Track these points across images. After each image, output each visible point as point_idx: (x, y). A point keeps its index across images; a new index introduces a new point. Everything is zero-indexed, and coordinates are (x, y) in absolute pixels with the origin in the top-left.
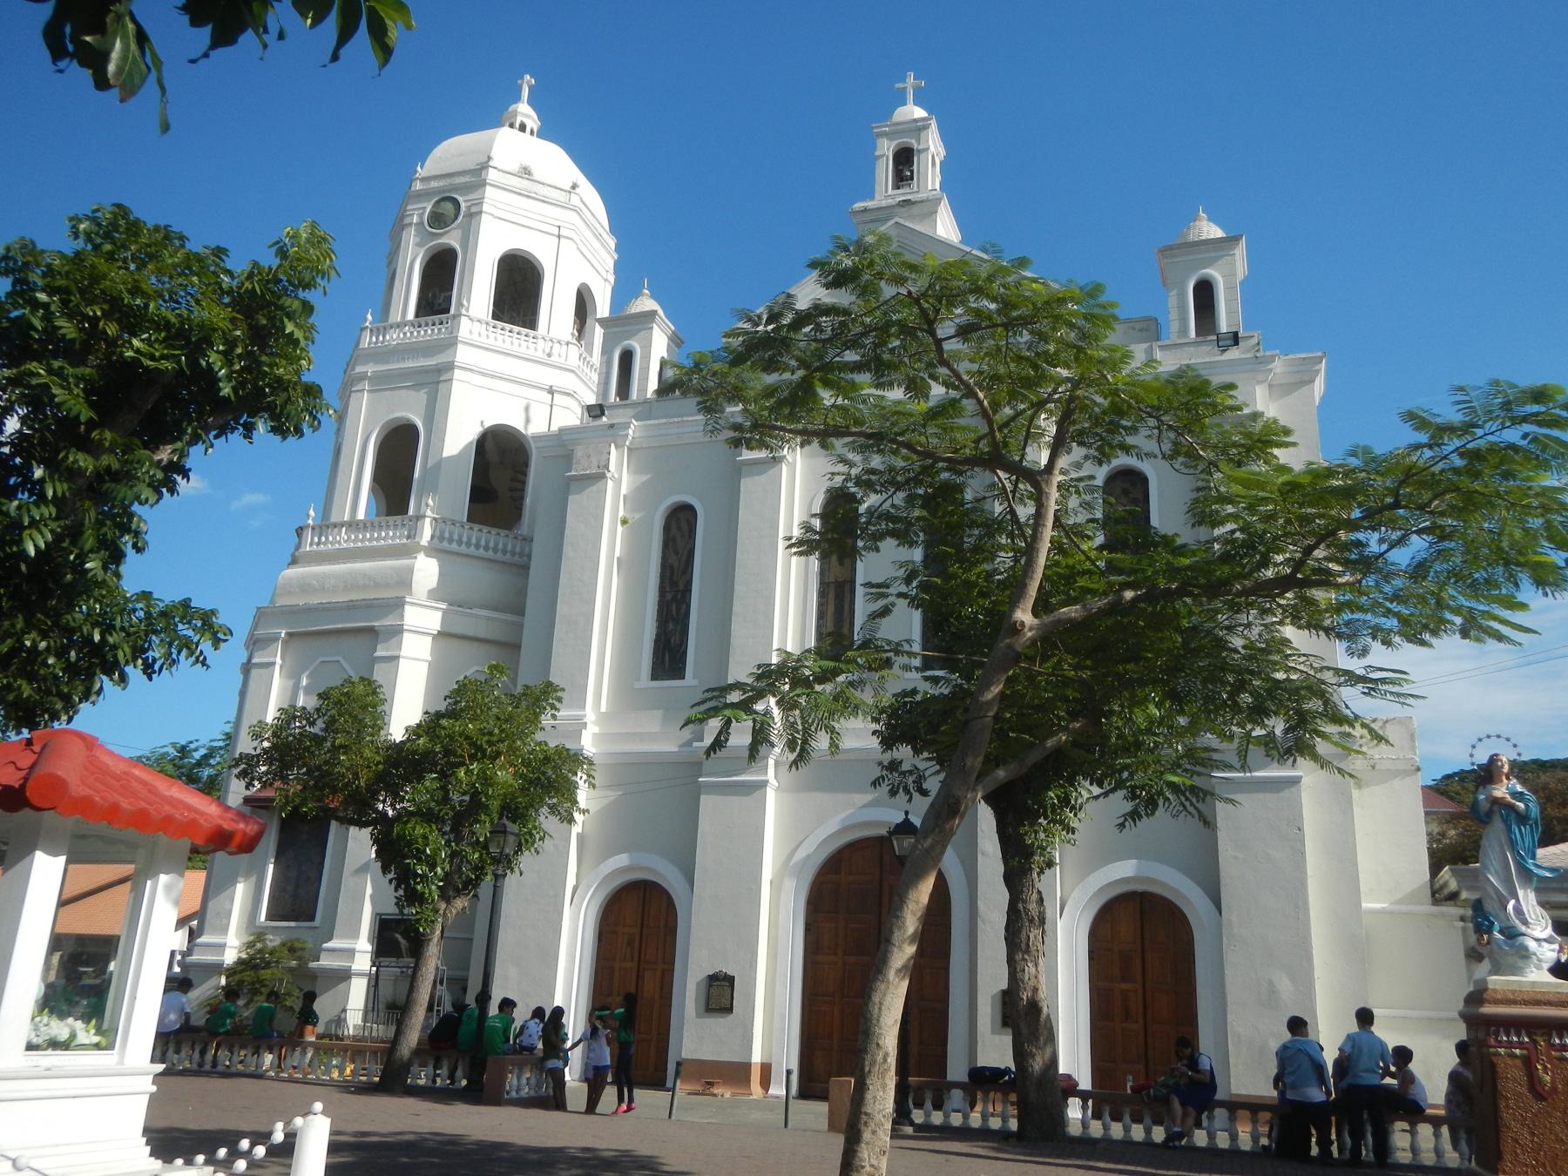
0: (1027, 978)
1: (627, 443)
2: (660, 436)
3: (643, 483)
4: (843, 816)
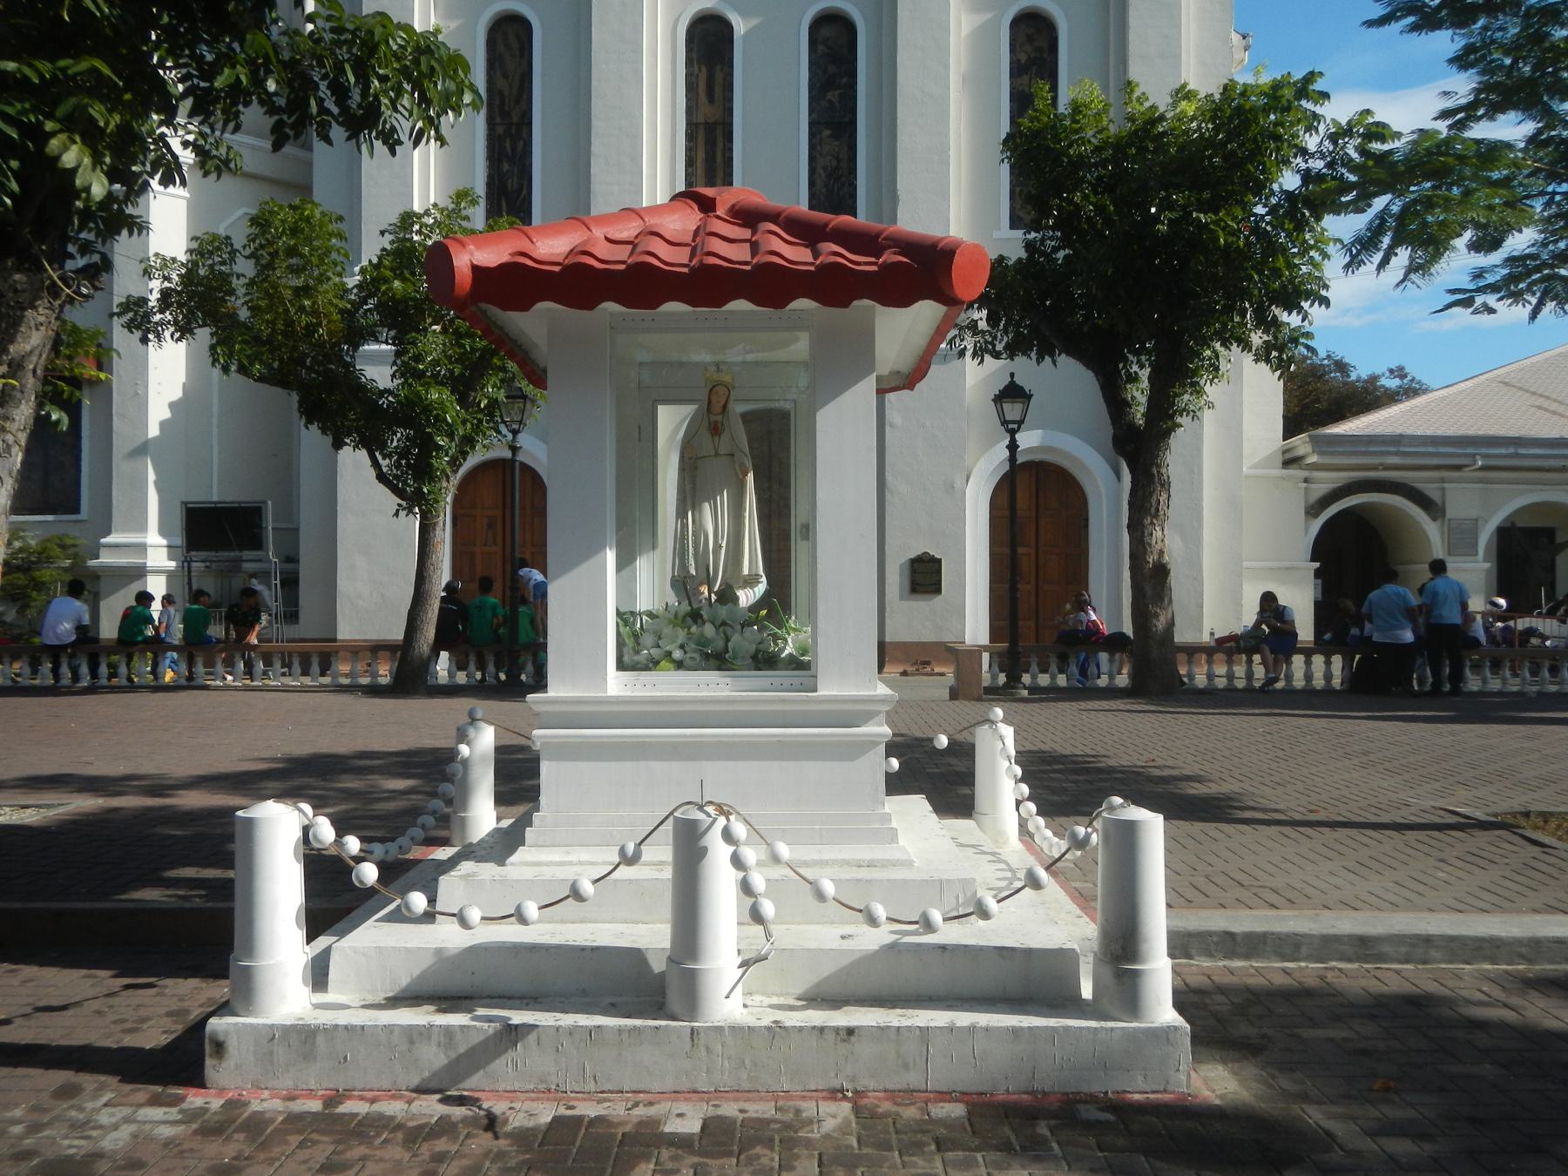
0: (1154, 542)
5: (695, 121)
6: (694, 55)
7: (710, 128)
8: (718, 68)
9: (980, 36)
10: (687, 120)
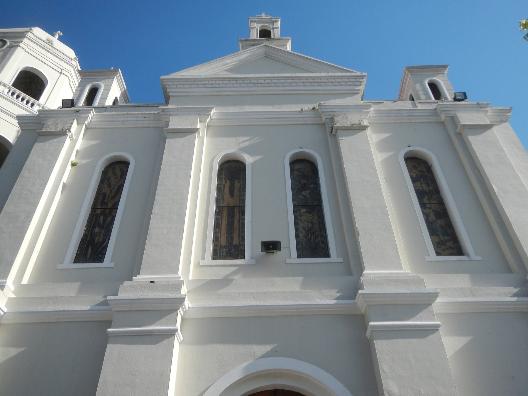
1: (86, 123)
4: (244, 365)
5: (222, 206)
6: (223, 176)
7: (231, 210)
8: (237, 181)
9: (388, 163)
10: (217, 204)
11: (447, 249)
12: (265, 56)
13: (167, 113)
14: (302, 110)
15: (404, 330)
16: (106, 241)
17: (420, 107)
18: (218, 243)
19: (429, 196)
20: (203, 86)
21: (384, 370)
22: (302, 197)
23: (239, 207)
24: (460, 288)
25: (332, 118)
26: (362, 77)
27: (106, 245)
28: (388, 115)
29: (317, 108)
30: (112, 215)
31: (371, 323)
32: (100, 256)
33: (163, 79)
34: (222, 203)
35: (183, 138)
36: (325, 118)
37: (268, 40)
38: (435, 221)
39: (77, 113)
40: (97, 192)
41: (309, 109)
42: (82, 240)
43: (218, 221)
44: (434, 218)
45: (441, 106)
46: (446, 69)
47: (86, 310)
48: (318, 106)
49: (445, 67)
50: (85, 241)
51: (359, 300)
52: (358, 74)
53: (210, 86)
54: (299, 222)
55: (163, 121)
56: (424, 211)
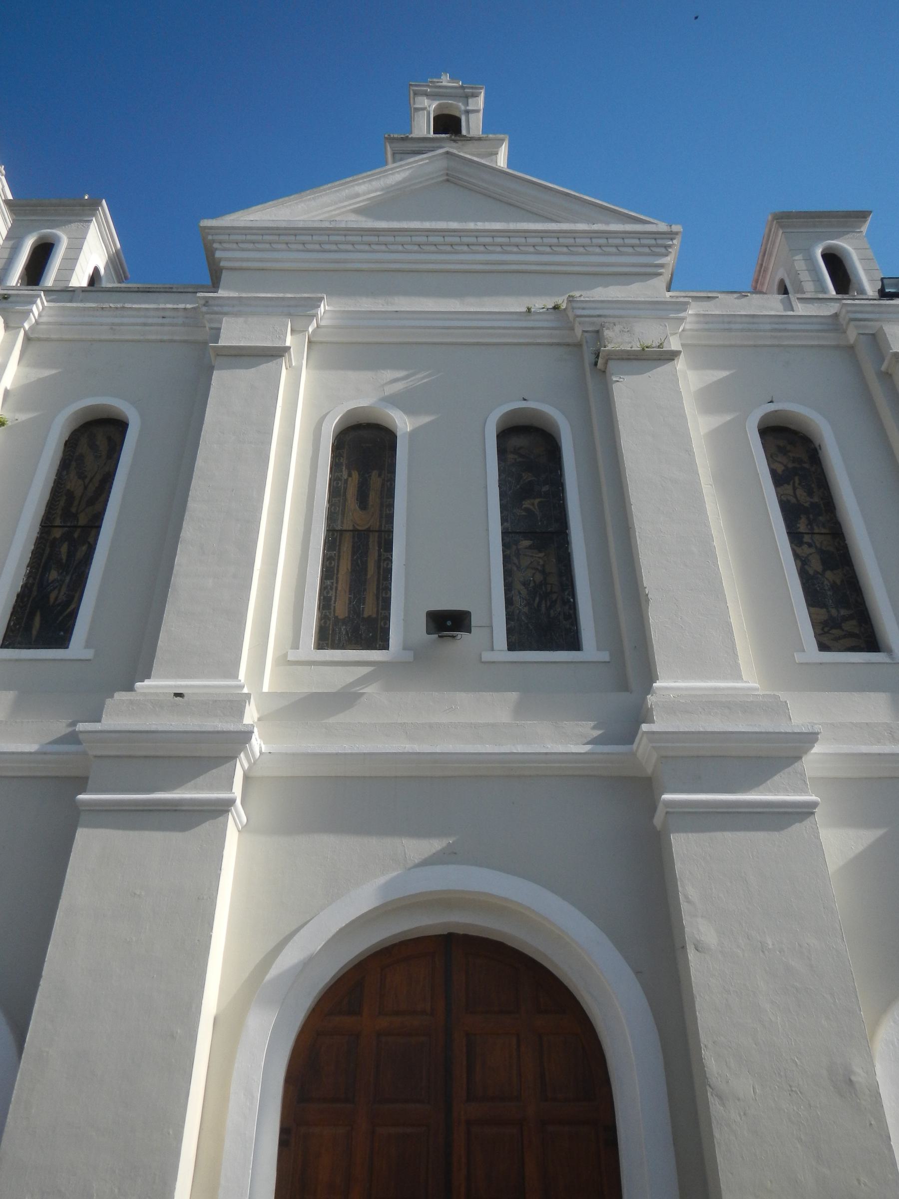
1: (27, 326)
2: (82, 324)
3: (41, 381)
4: (382, 880)
5: (339, 528)
6: (344, 461)
7: (360, 537)
8: (375, 473)
11: (845, 637)
12: (445, 178)
13: (215, 309)
14: (529, 309)
15: (738, 813)
16: (76, 599)
17: (801, 309)
18: (330, 613)
19: (811, 516)
20: (301, 247)
21: (690, 897)
22: (524, 513)
23: (380, 531)
24: (867, 724)
25: (597, 332)
26: (671, 235)
27: (74, 609)
28: (727, 326)
29: (564, 306)
30: (89, 543)
31: (667, 797)
32: (62, 633)
33: (205, 228)
34: (339, 522)
35: (253, 370)
36: (581, 331)
37: (455, 141)
38: (821, 574)
39: (5, 301)
40: (53, 487)
41: (544, 310)
42: (21, 597)
43: (330, 563)
44: (819, 568)
45: (849, 309)
46: (865, 222)
47: (30, 753)
48: (565, 301)
49: (862, 215)
50: (26, 599)
51: (642, 747)
52: (662, 227)
53: (317, 247)
54: (515, 568)
55: (205, 327)
56: (799, 551)
